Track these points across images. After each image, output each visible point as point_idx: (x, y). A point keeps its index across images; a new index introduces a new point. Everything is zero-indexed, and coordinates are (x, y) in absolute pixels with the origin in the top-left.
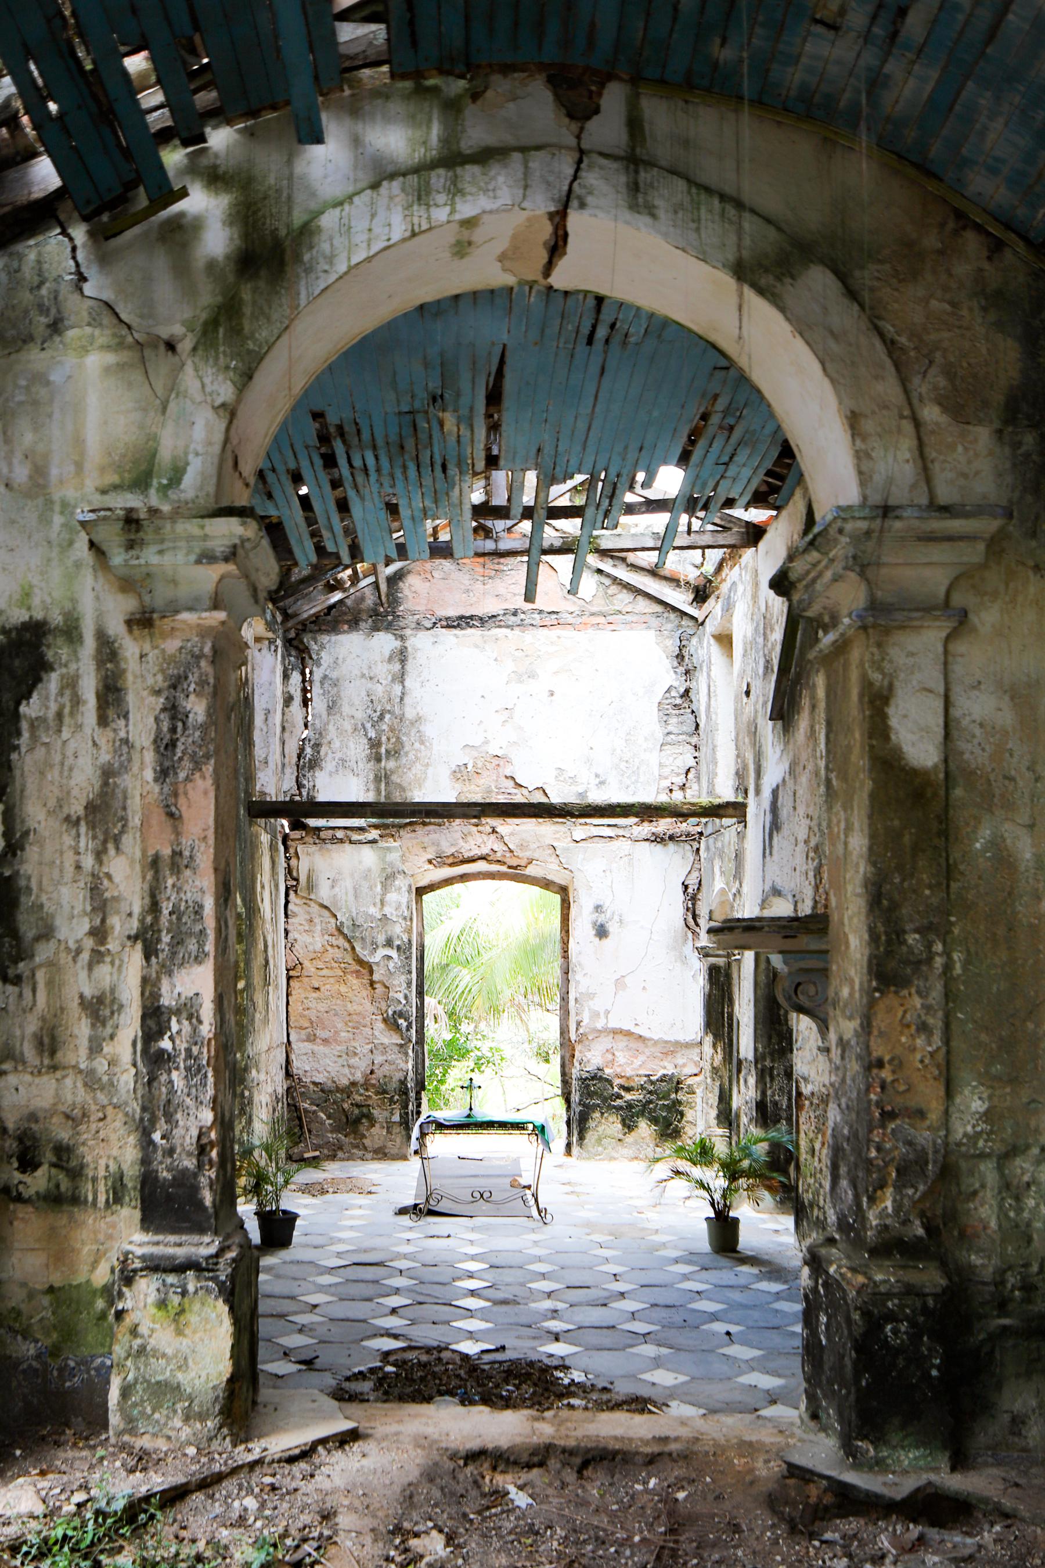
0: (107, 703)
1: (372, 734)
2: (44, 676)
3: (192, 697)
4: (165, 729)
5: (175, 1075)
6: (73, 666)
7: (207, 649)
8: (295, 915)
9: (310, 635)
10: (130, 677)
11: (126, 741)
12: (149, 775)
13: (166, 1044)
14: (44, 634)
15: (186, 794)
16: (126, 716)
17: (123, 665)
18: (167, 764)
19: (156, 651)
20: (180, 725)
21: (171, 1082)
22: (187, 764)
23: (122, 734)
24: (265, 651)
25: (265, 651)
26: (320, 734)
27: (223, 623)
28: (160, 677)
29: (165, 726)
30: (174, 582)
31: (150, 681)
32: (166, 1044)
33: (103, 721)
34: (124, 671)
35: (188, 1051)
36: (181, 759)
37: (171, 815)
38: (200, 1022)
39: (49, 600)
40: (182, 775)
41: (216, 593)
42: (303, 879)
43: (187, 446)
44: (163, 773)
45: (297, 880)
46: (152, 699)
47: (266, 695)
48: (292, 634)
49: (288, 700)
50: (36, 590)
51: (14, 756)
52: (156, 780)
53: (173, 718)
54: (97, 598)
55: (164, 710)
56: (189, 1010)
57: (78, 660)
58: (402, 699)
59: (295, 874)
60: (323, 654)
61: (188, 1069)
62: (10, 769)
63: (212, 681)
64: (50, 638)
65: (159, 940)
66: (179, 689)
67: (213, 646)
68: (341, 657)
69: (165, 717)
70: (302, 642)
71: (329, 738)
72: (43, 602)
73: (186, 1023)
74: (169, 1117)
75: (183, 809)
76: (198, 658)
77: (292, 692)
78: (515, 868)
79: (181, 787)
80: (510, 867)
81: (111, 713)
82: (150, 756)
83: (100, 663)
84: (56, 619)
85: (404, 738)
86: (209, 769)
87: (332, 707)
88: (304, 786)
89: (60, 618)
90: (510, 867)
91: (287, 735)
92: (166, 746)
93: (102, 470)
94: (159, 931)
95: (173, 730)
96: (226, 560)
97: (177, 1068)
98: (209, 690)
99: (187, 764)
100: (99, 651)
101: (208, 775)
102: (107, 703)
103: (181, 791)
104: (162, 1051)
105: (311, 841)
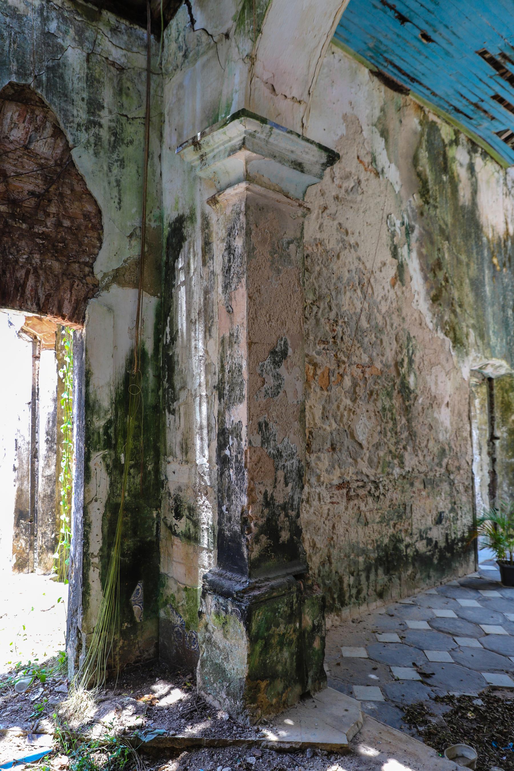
0: (206, 252)
2: (183, 244)
3: (237, 238)
4: (226, 261)
5: (231, 471)
6: (193, 236)
7: (243, 208)
10: (214, 235)
11: (213, 272)
12: (220, 290)
13: (227, 452)
14: (183, 221)
15: (235, 298)
16: (213, 258)
17: (212, 229)
18: (227, 282)
19: (222, 216)
20: (232, 256)
21: (230, 475)
22: (235, 280)
23: (211, 268)
27: (247, 189)
28: (224, 231)
29: (226, 258)
30: (228, 173)
31: (220, 235)
32: (227, 452)
33: (204, 263)
34: (212, 232)
35: (236, 456)
36: (233, 277)
37: (229, 312)
38: (241, 439)
39: (184, 203)
40: (233, 287)
41: (247, 171)
43: (233, 89)
44: (226, 287)
46: (221, 245)
50: (180, 199)
51: (173, 290)
52: (223, 293)
53: (229, 253)
54: (201, 194)
55: (226, 249)
56: (236, 431)
57: (195, 232)
61: (237, 469)
62: (172, 298)
63: (245, 226)
64: (185, 223)
65: (224, 388)
66: (231, 236)
67: (246, 204)
69: (226, 254)
72: (182, 204)
73: (235, 439)
74: (229, 496)
75: (234, 307)
76: (238, 214)
79: (233, 294)
81: (207, 257)
82: (220, 279)
83: (203, 230)
84: (187, 212)
86: (244, 280)
89: (188, 211)
92: (227, 271)
93: (202, 122)
94: (225, 383)
95: (229, 261)
96: (240, 149)
97: (232, 468)
98: (244, 232)
99: (235, 280)
100: (202, 224)
101: (244, 285)
102: (206, 252)
103: (233, 297)
104: (226, 456)
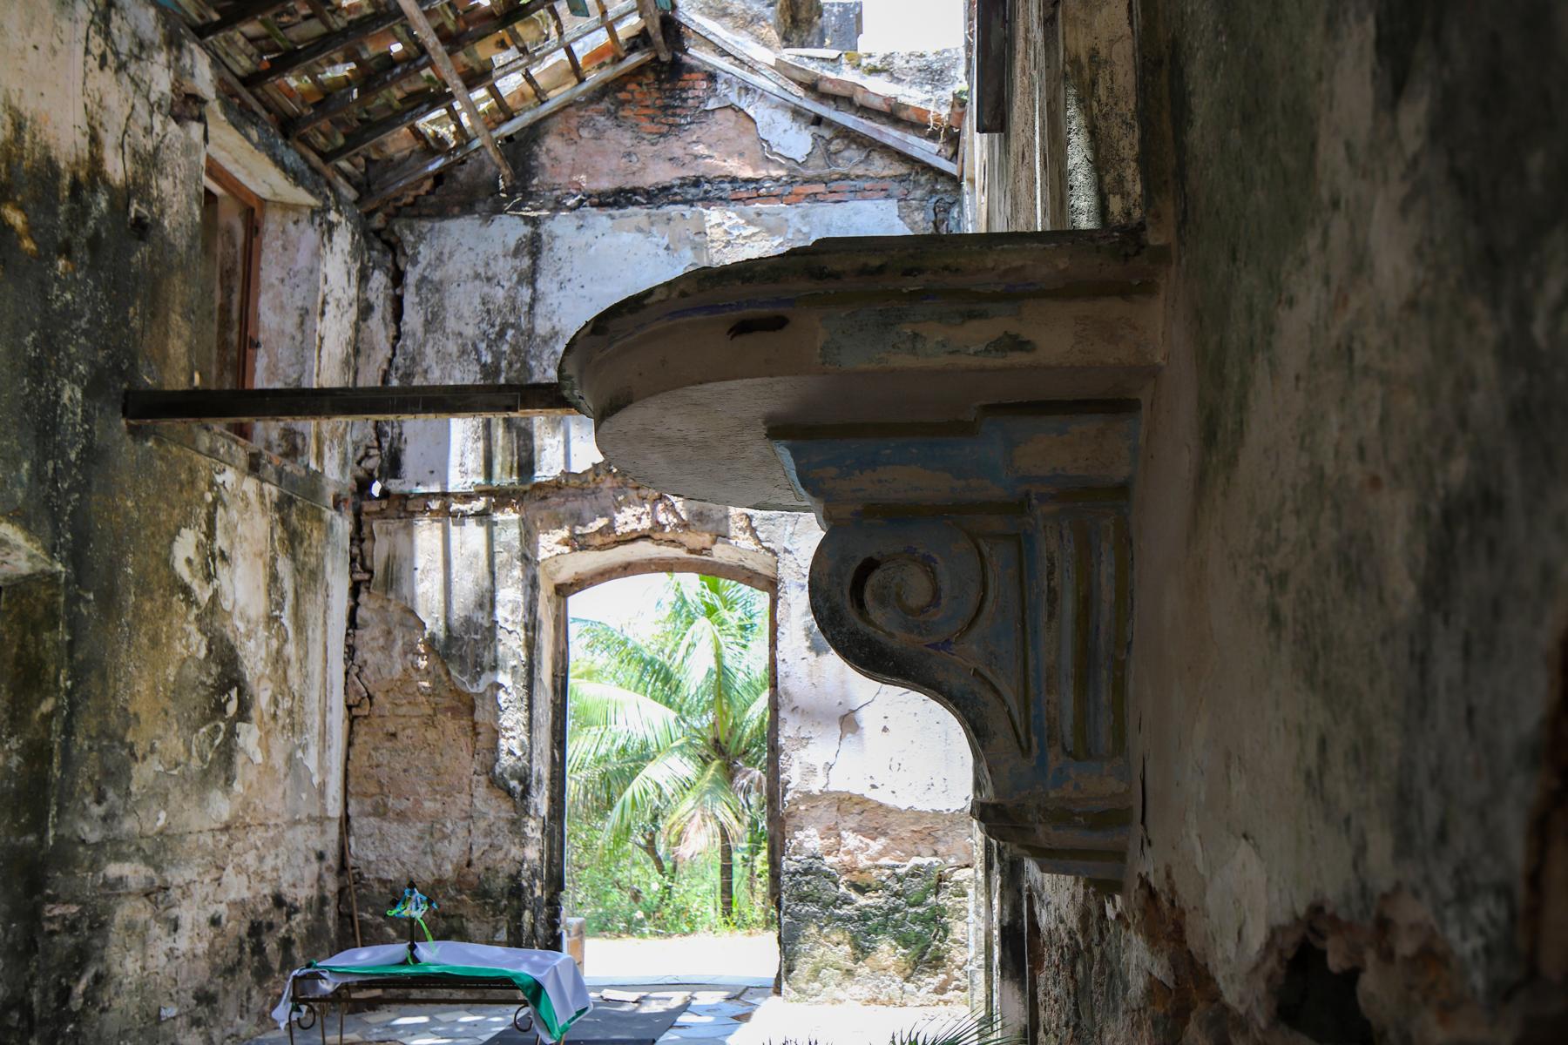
1: (487, 358)
8: (366, 625)
9: (403, 221)
24: (304, 225)
25: (304, 225)
26: (413, 359)
42: (378, 568)
45: (371, 572)
47: (304, 287)
48: (378, 221)
49: (365, 310)
58: (531, 307)
59: (368, 563)
60: (421, 248)
68: (446, 251)
70: (393, 232)
71: (425, 365)
77: (372, 297)
78: (699, 552)
80: (691, 551)
85: (533, 363)
87: (433, 322)
88: (385, 434)
90: (691, 551)
91: (361, 360)
105: (394, 513)
